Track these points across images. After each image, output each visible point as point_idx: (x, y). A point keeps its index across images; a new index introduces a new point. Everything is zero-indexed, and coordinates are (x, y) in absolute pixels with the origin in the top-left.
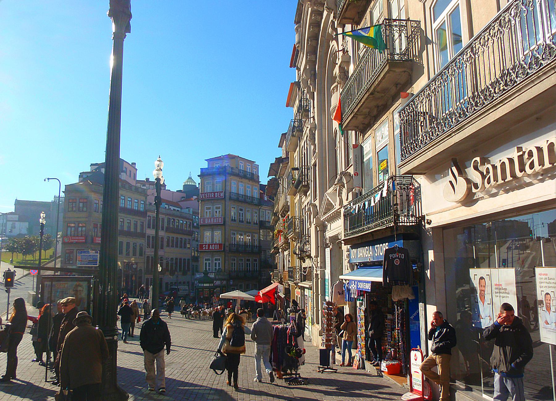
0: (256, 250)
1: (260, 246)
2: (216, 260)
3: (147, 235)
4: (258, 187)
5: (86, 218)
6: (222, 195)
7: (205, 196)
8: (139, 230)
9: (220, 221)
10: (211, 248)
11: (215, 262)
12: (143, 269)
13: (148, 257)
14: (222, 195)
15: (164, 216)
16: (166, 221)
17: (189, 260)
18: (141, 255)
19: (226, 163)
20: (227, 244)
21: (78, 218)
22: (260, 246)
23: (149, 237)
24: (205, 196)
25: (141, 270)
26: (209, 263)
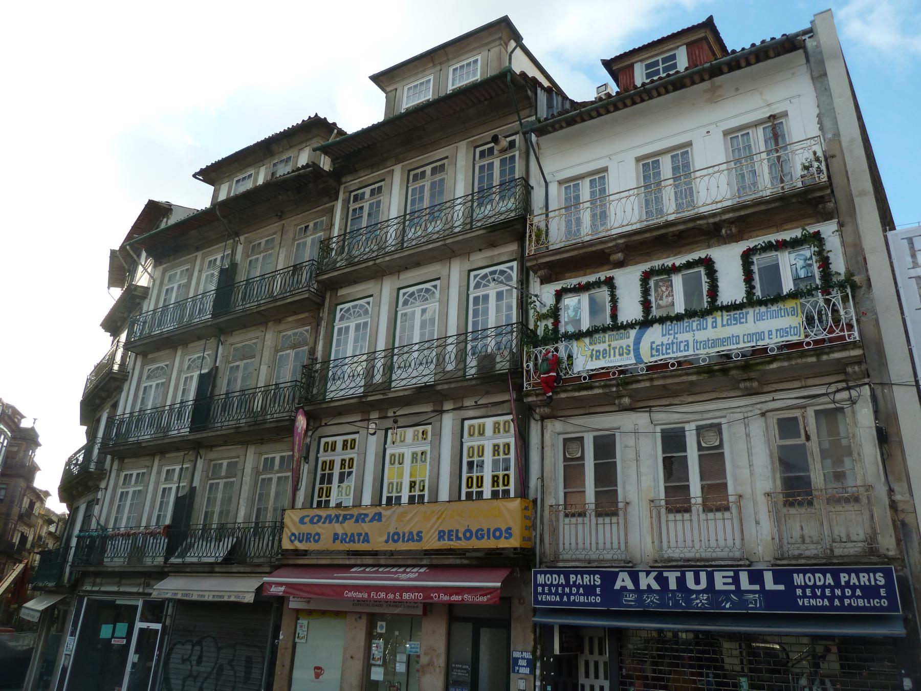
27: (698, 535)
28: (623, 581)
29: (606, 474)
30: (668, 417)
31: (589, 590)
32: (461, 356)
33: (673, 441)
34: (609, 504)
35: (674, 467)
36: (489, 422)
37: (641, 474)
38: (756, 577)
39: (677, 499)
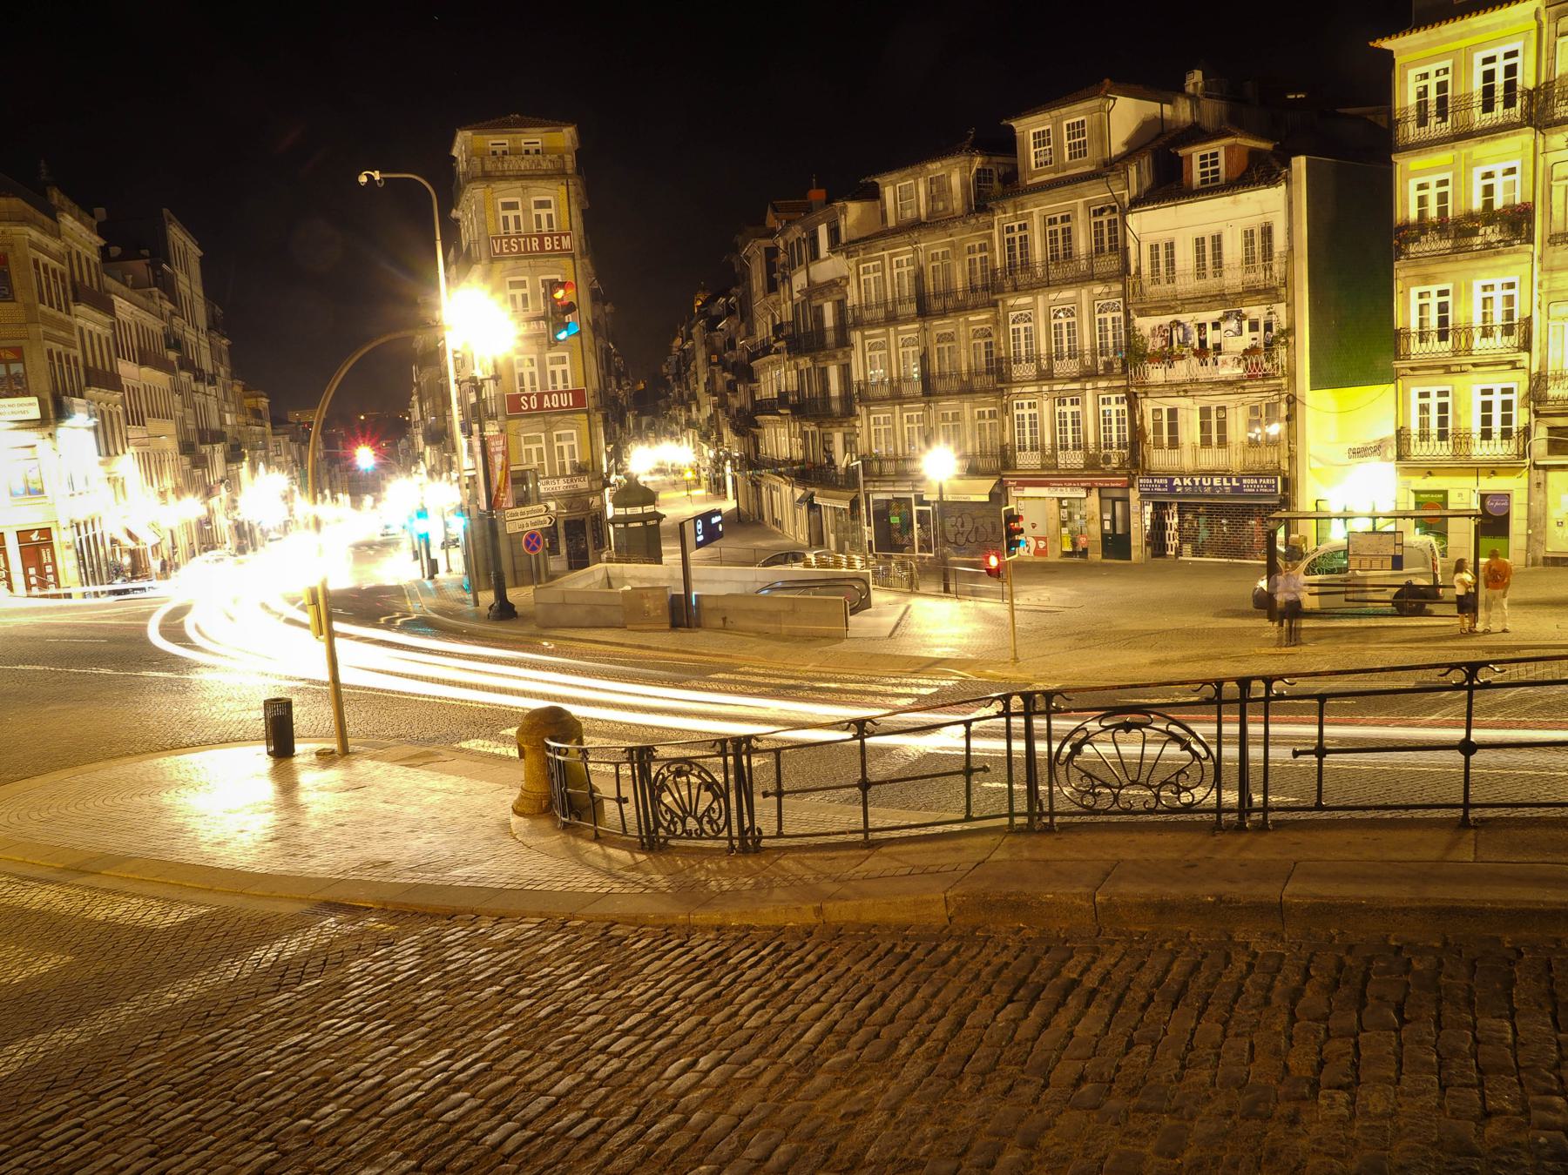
2: (559, 438)
6: (566, 242)
7: (509, 247)
10: (546, 404)
11: (557, 444)
24: (509, 247)
26: (540, 451)
27: (1211, 459)
28: (1177, 481)
29: (1173, 428)
30: (1204, 402)
31: (1163, 486)
32: (1095, 361)
33: (1205, 412)
34: (1174, 443)
35: (1205, 427)
36: (1113, 397)
37: (1190, 431)
38: (1229, 480)
39: (1206, 442)
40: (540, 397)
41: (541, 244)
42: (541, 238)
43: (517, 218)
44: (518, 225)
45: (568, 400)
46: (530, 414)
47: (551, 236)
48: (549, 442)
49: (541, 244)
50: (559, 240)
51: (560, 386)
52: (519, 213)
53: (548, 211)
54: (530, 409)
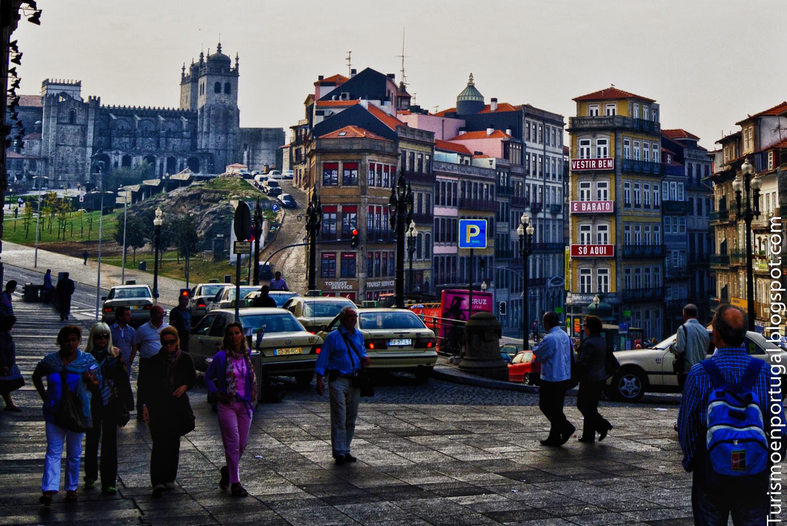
0: (658, 251)
1: (663, 247)
3: (435, 217)
4: (659, 145)
5: (358, 196)
7: (580, 165)
8: (424, 211)
9: (609, 208)
10: (592, 252)
12: (430, 281)
13: (437, 258)
14: (610, 164)
15: (457, 179)
16: (459, 187)
17: (491, 258)
18: (427, 256)
19: (613, 109)
20: (620, 246)
21: (342, 197)
22: (663, 247)
23: (437, 220)
24: (580, 165)
25: (427, 283)
40: (589, 248)
41: (597, 165)
42: (597, 161)
43: (588, 149)
44: (588, 153)
45: (602, 251)
46: (583, 259)
47: (602, 160)
48: (593, 273)
49: (597, 165)
50: (606, 163)
51: (603, 244)
52: (590, 146)
53: (604, 146)
54: (583, 254)
